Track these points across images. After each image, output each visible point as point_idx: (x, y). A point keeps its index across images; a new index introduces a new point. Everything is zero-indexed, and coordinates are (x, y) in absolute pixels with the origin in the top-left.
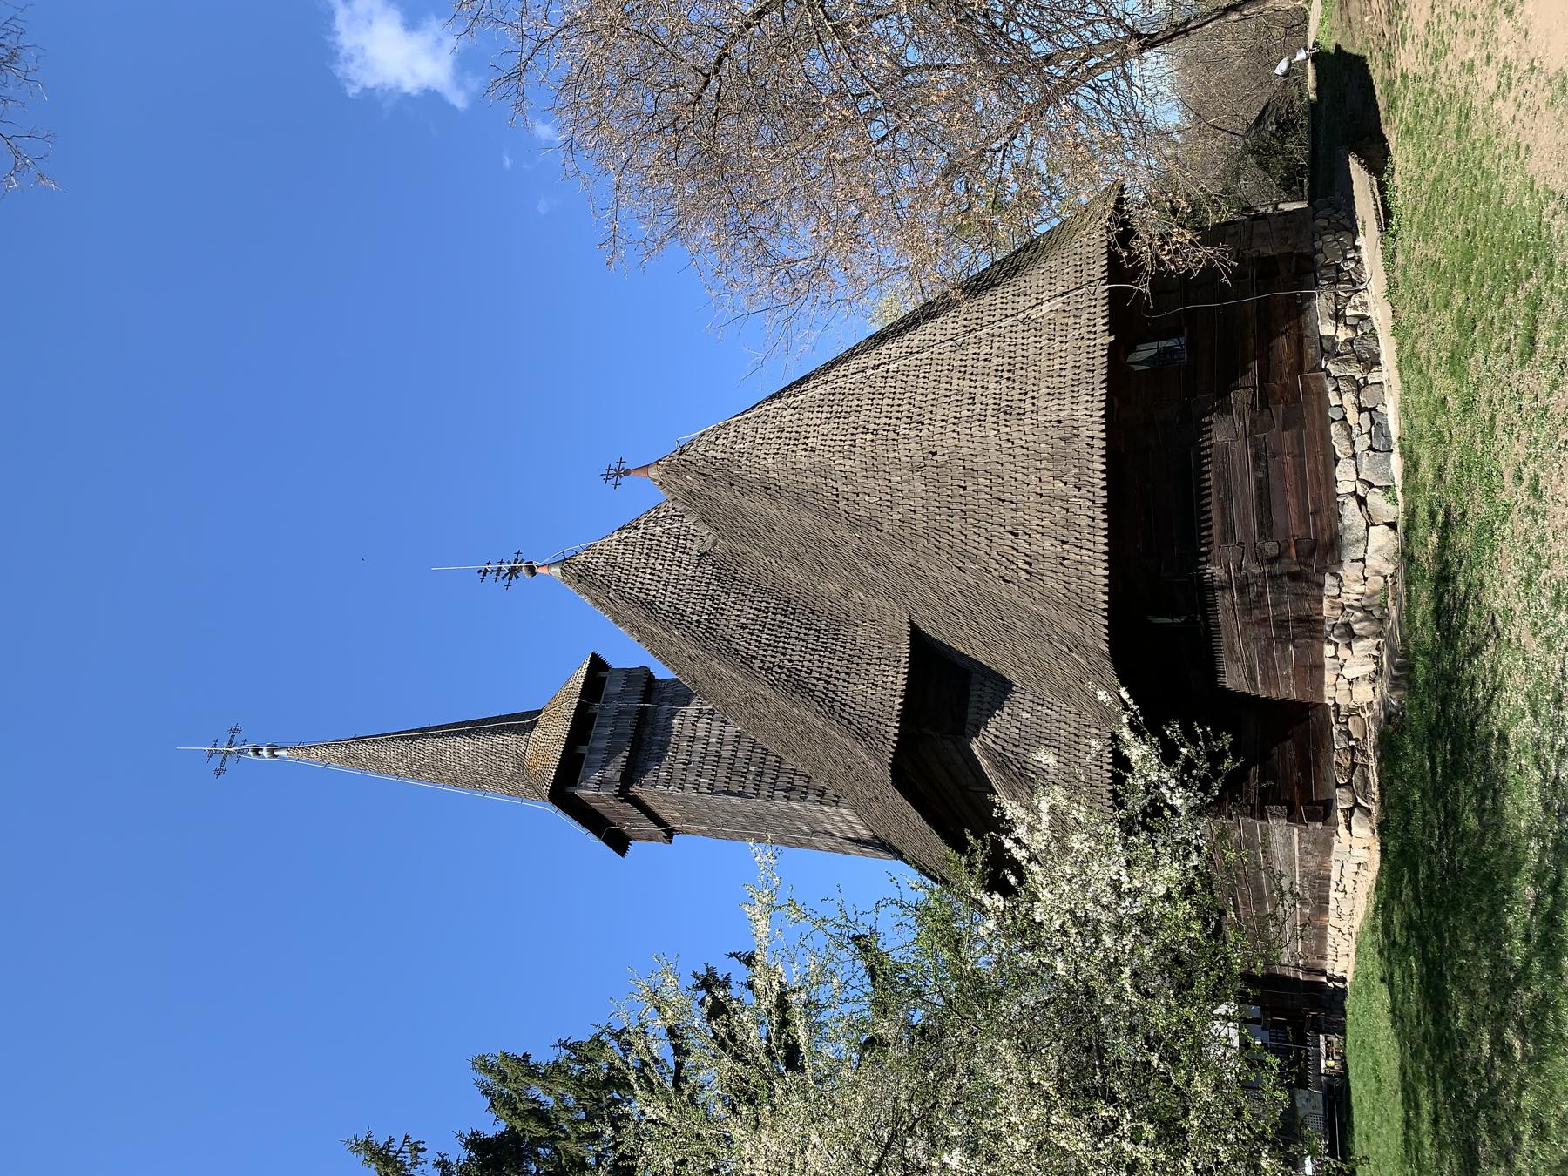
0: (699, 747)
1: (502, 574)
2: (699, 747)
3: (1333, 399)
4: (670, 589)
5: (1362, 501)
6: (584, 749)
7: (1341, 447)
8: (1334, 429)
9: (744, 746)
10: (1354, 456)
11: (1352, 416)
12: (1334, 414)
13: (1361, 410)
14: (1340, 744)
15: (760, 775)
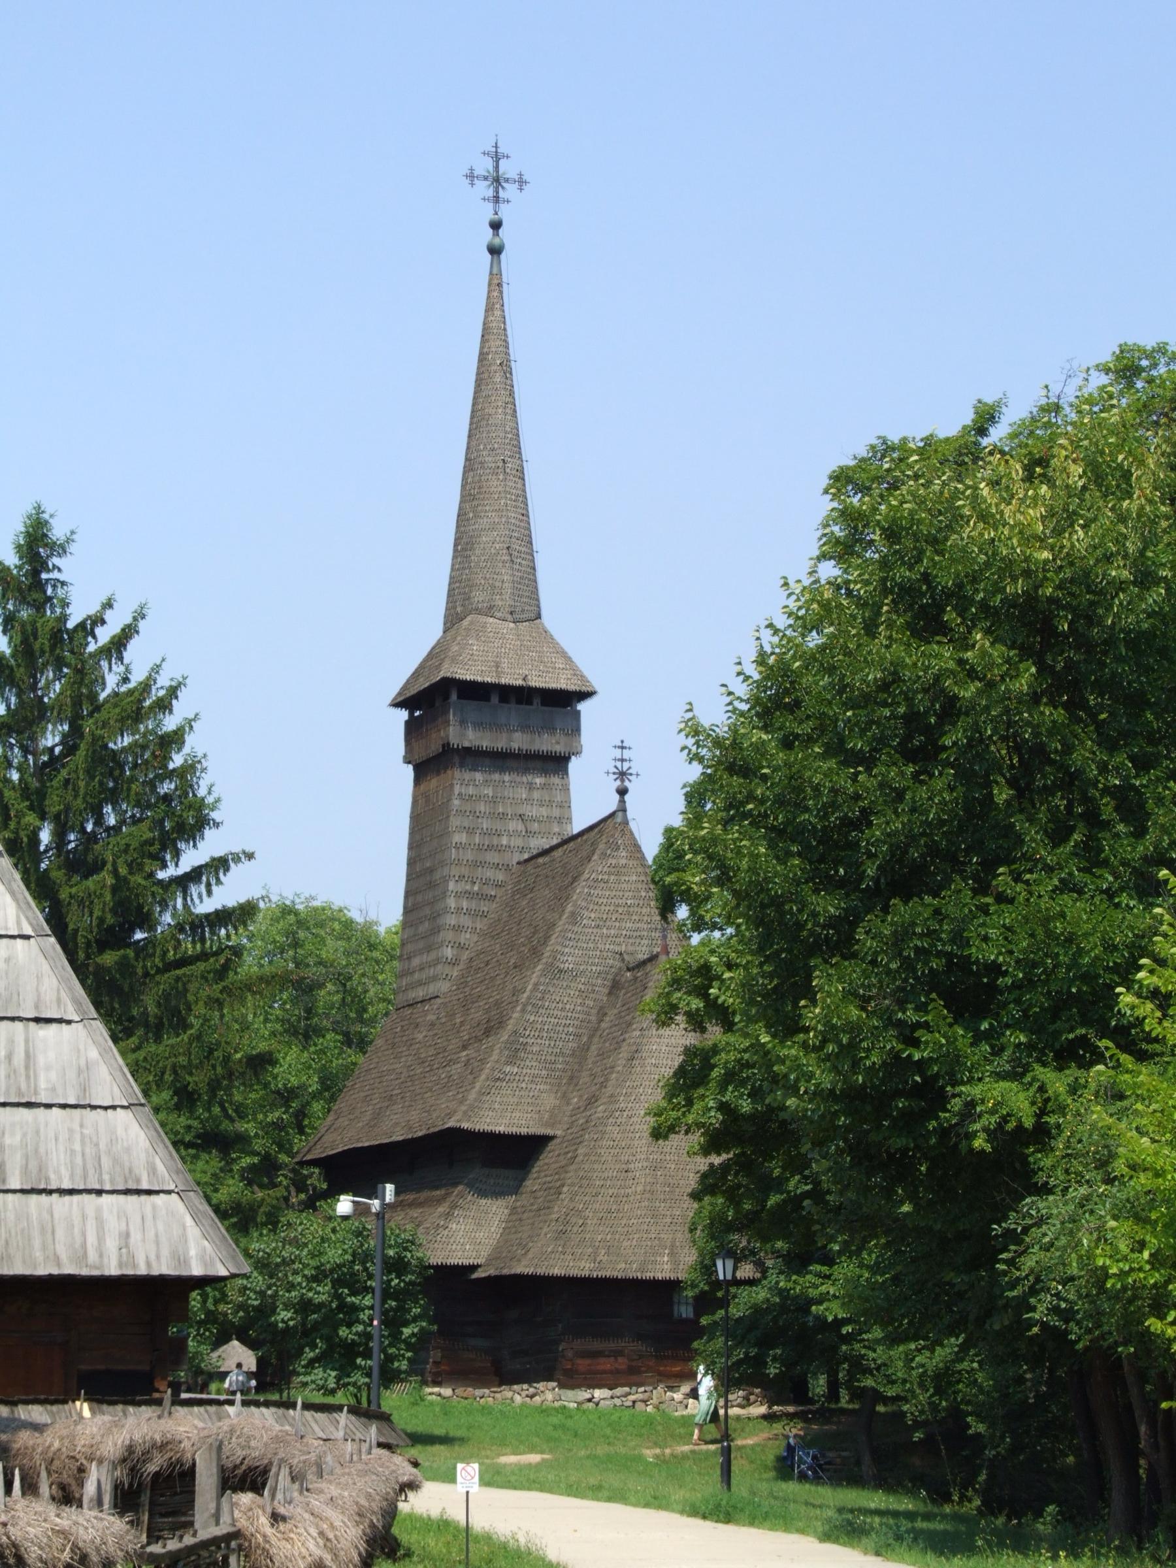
0: (498, 825)
1: (619, 764)
2: (498, 825)
3: (641, 1389)
4: (595, 931)
5: (590, 1400)
6: (495, 699)
7: (619, 1391)
8: (627, 1389)
9: (500, 876)
10: (612, 1397)
11: (632, 1398)
12: (634, 1388)
13: (634, 1402)
14: (478, 1392)
15: (469, 895)
